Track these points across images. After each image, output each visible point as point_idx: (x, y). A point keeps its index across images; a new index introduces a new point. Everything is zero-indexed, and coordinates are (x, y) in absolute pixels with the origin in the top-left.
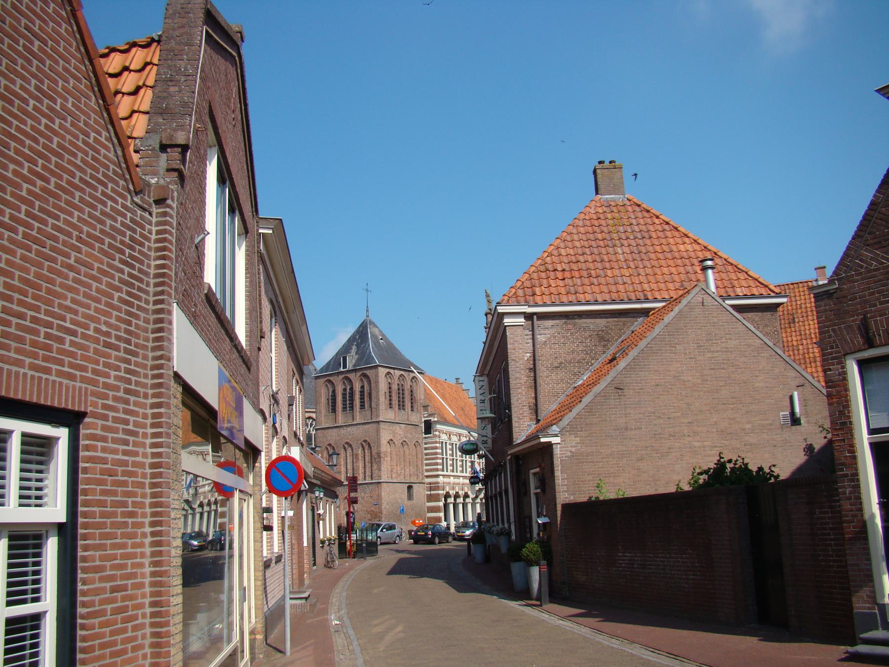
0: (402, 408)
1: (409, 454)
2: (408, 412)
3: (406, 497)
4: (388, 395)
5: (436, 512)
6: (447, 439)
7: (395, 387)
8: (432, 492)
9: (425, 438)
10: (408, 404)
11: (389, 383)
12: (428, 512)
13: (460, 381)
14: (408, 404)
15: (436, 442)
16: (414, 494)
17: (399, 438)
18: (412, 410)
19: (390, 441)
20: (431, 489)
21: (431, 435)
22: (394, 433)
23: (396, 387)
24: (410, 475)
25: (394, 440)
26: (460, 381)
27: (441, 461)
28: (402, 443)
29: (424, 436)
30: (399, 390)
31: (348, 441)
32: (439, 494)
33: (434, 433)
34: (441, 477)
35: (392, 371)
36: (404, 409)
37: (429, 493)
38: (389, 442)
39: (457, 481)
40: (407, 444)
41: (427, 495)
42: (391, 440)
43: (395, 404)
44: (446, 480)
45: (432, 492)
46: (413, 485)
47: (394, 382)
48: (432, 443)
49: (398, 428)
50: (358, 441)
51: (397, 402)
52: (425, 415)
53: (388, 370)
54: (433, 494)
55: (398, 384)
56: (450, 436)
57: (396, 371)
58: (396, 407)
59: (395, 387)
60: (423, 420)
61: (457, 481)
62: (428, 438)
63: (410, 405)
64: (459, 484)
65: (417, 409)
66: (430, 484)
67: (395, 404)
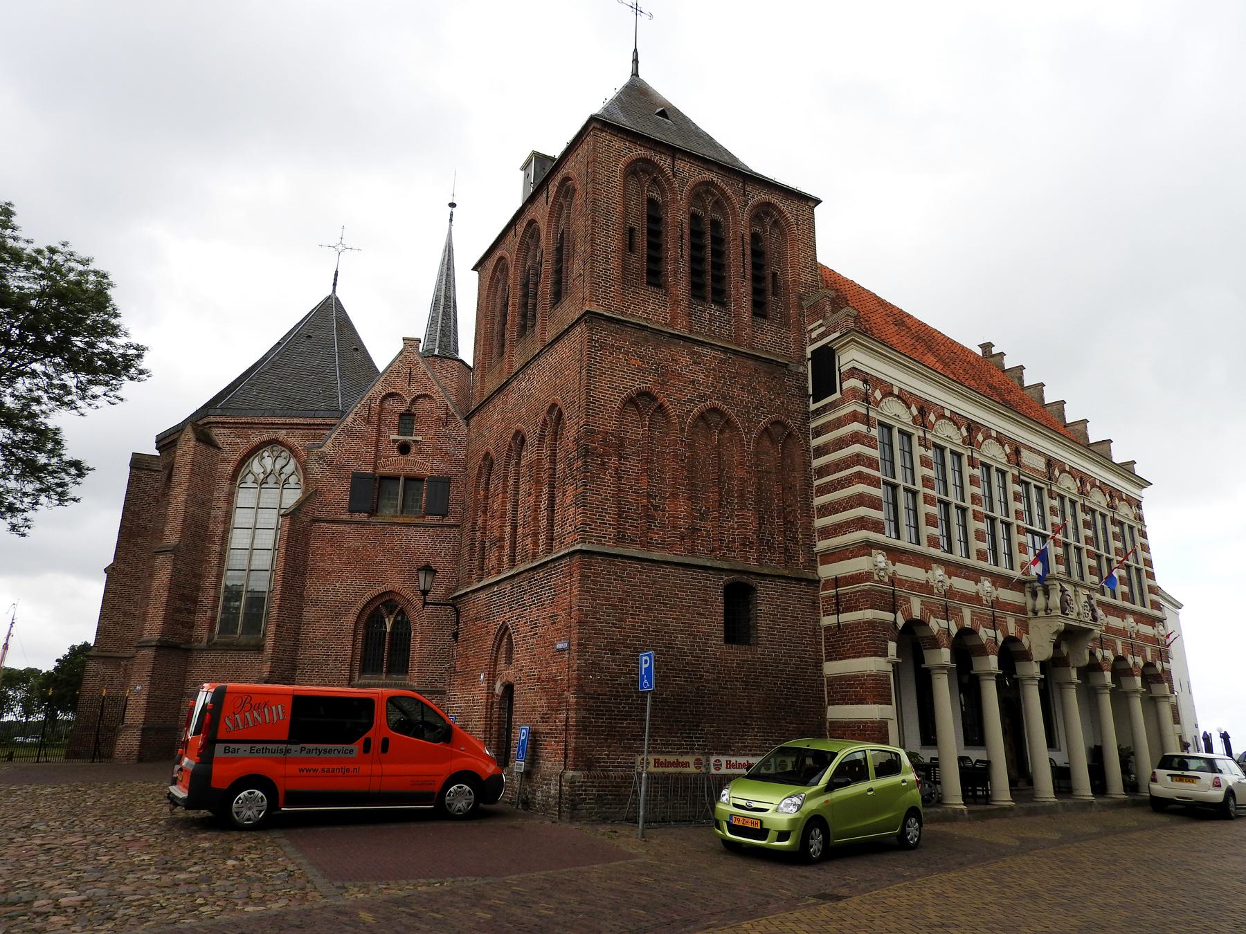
0: (709, 296)
1: (741, 464)
2: (737, 315)
3: (719, 629)
4: (642, 240)
5: (861, 701)
6: (906, 418)
7: (677, 215)
8: (846, 617)
9: (818, 412)
10: (740, 288)
11: (651, 202)
12: (832, 702)
13: (995, 351)
14: (740, 288)
15: (854, 417)
16: (763, 624)
17: (689, 392)
18: (759, 309)
19: (640, 401)
20: (840, 605)
21: (837, 395)
22: (664, 374)
23: (684, 218)
24: (744, 545)
25: (663, 399)
26: (995, 351)
27: (879, 492)
28: (702, 416)
29: (813, 407)
30: (696, 234)
31: (519, 425)
32: (872, 624)
33: (846, 385)
34: (880, 559)
35: (664, 162)
36: (723, 304)
37: (828, 620)
38: (630, 401)
39: (962, 584)
40: (729, 422)
41: (828, 628)
42: (645, 394)
43: (675, 272)
44: (905, 571)
45: (846, 617)
46: (754, 581)
47: (674, 201)
48: (839, 423)
49: (685, 359)
50: (537, 414)
51: (685, 266)
52: (814, 335)
53: (641, 152)
54: (847, 626)
55: (694, 218)
56: (923, 411)
57: (682, 165)
58: (682, 287)
59: (677, 215)
60: (809, 350)
61: (962, 584)
62: (824, 409)
63: (746, 288)
64: (976, 599)
65: (786, 317)
66: (837, 582)
67: (675, 272)
